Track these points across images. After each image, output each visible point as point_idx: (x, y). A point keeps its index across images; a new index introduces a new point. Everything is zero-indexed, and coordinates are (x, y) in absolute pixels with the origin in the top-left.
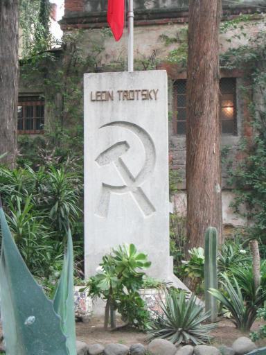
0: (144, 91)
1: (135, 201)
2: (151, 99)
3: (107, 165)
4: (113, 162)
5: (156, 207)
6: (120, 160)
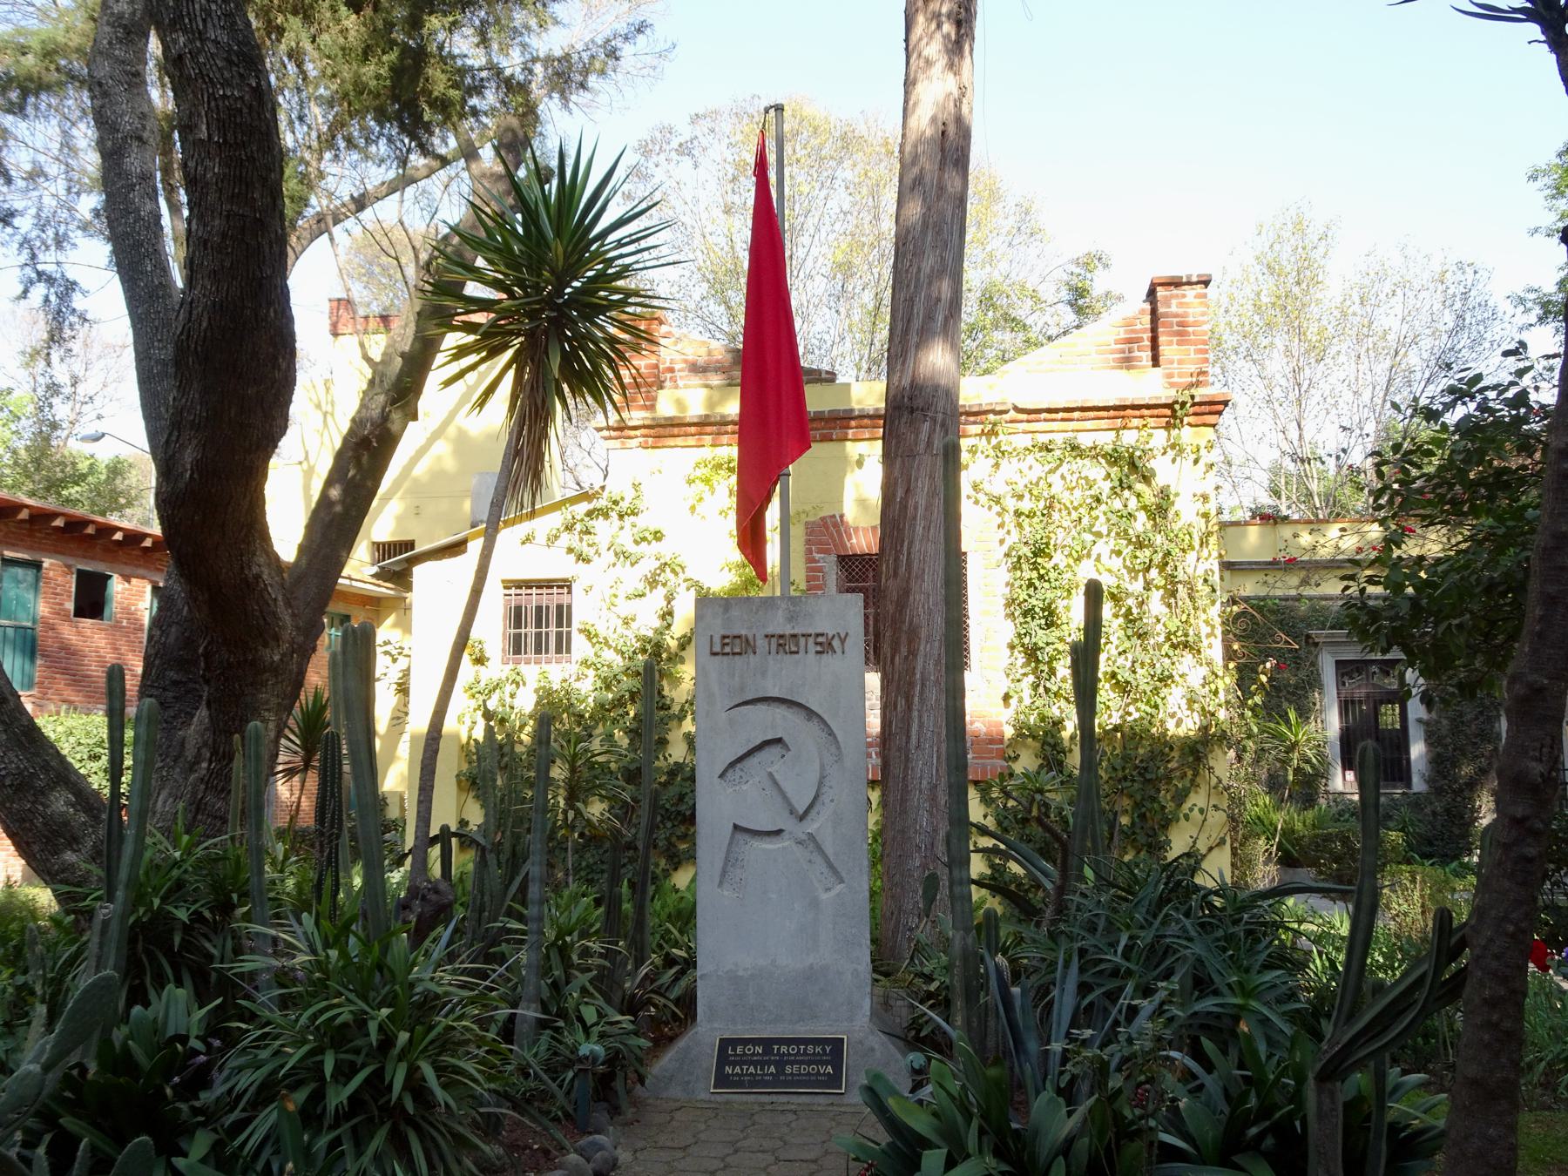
0: (818, 635)
3: (745, 787)
5: (844, 874)
6: (771, 775)
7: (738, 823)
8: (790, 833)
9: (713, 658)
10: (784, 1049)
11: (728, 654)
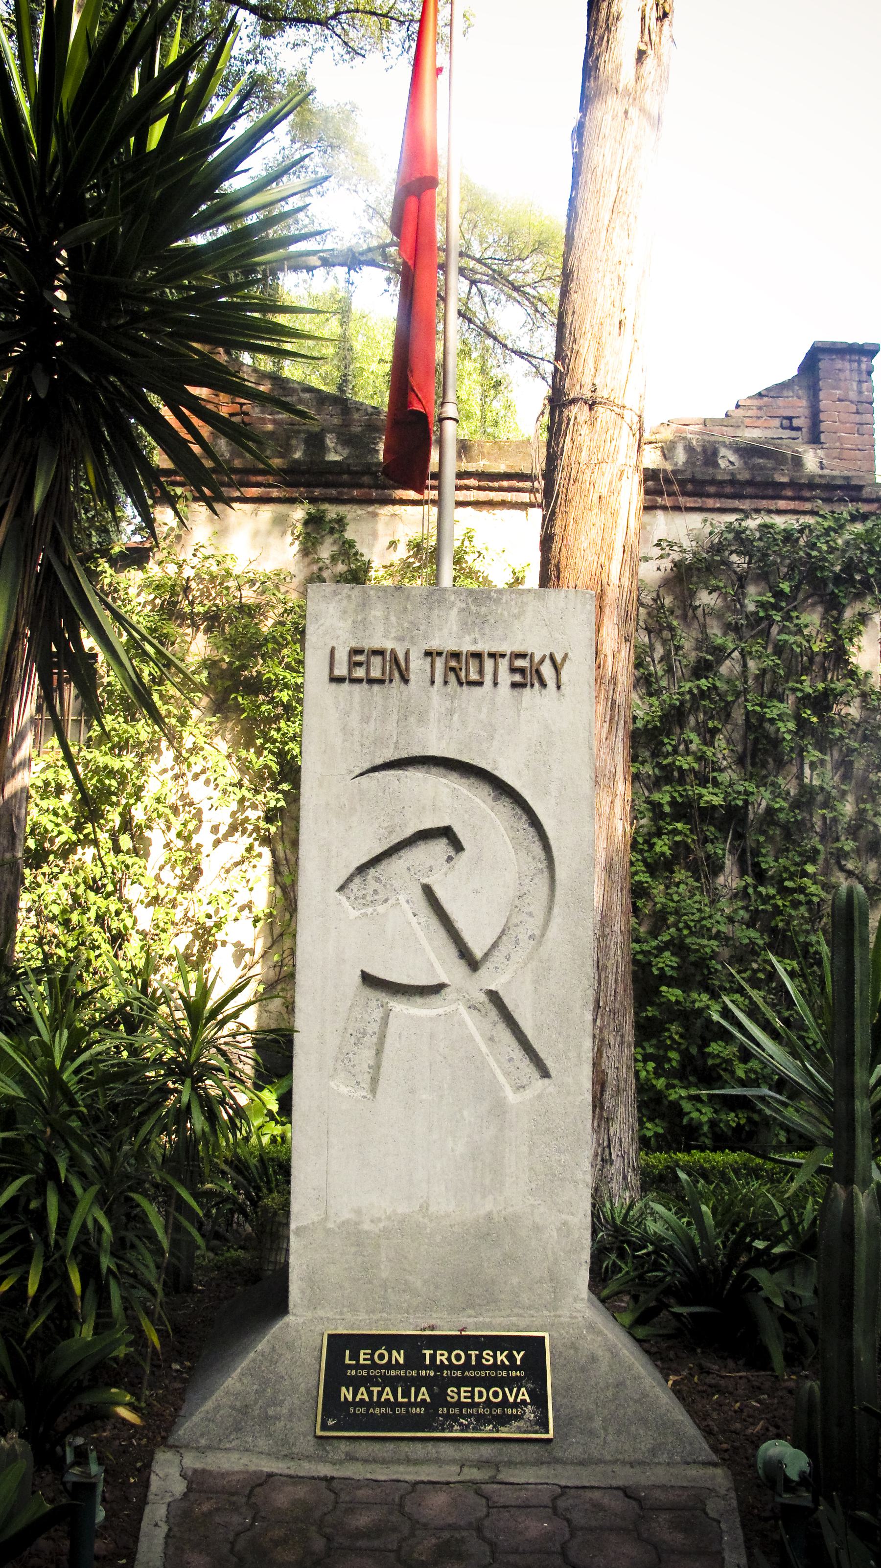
1: (478, 1038)
2: (543, 684)
3: (381, 909)
4: (402, 898)
5: (549, 1063)
6: (428, 891)
7: (368, 970)
8: (459, 991)
9: (334, 685)
10: (442, 1357)
11: (359, 681)
